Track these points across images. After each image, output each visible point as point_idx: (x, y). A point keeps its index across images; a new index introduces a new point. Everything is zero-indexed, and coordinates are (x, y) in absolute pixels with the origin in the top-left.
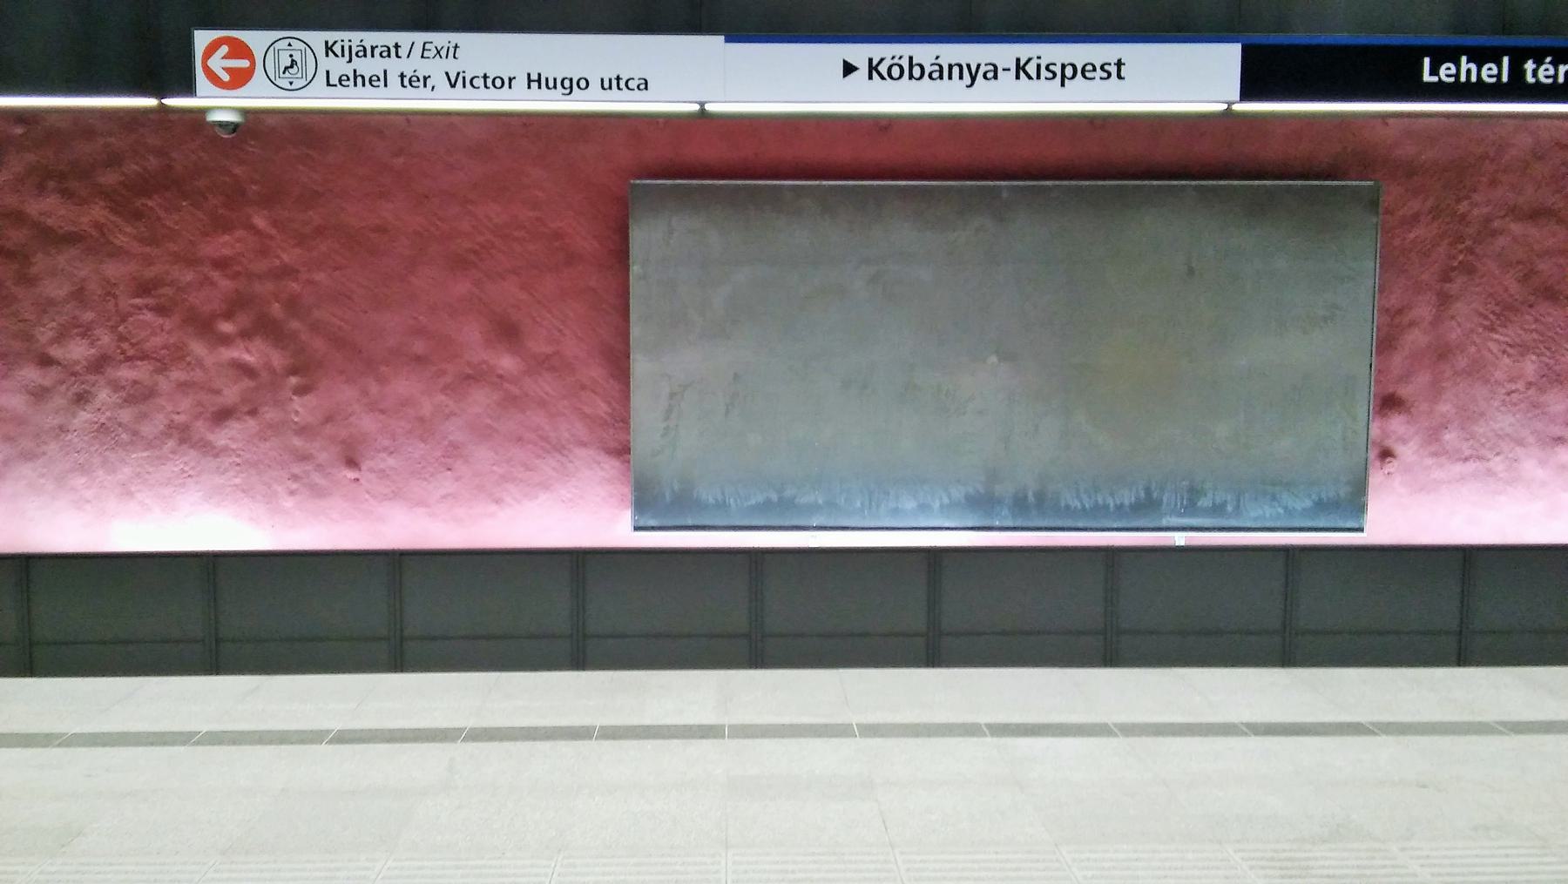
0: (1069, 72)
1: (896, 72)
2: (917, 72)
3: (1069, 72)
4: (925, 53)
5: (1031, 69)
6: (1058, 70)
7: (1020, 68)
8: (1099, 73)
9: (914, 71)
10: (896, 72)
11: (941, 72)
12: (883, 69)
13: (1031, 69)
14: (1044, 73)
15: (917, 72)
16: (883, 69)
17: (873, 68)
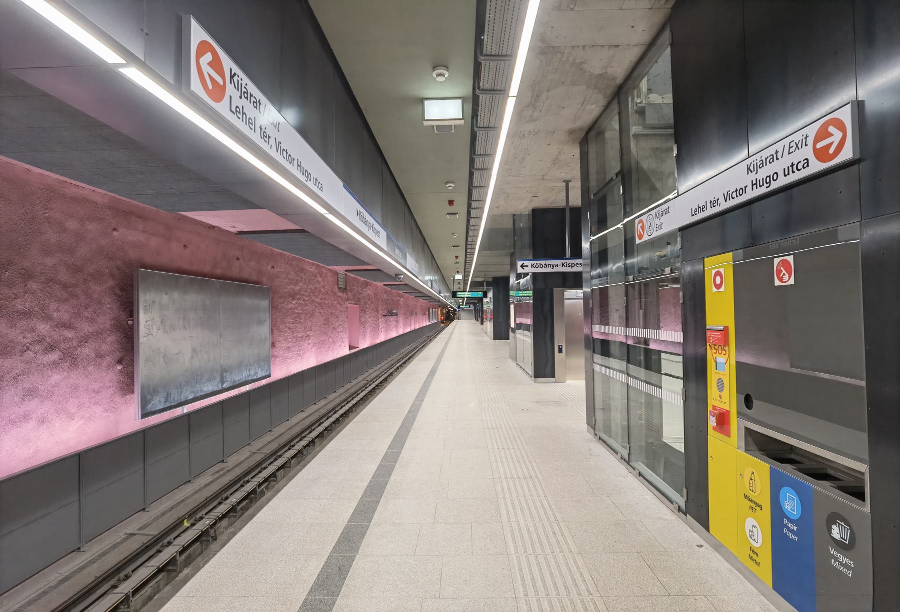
0: (573, 265)
1: (537, 266)
2: (541, 266)
3: (573, 265)
4: (543, 262)
5: (565, 265)
6: (570, 265)
7: (563, 265)
8: (579, 265)
9: (541, 266)
10: (537, 266)
11: (546, 266)
12: (534, 266)
13: (565, 265)
14: (568, 266)
15: (541, 266)
16: (534, 266)
17: (532, 266)
